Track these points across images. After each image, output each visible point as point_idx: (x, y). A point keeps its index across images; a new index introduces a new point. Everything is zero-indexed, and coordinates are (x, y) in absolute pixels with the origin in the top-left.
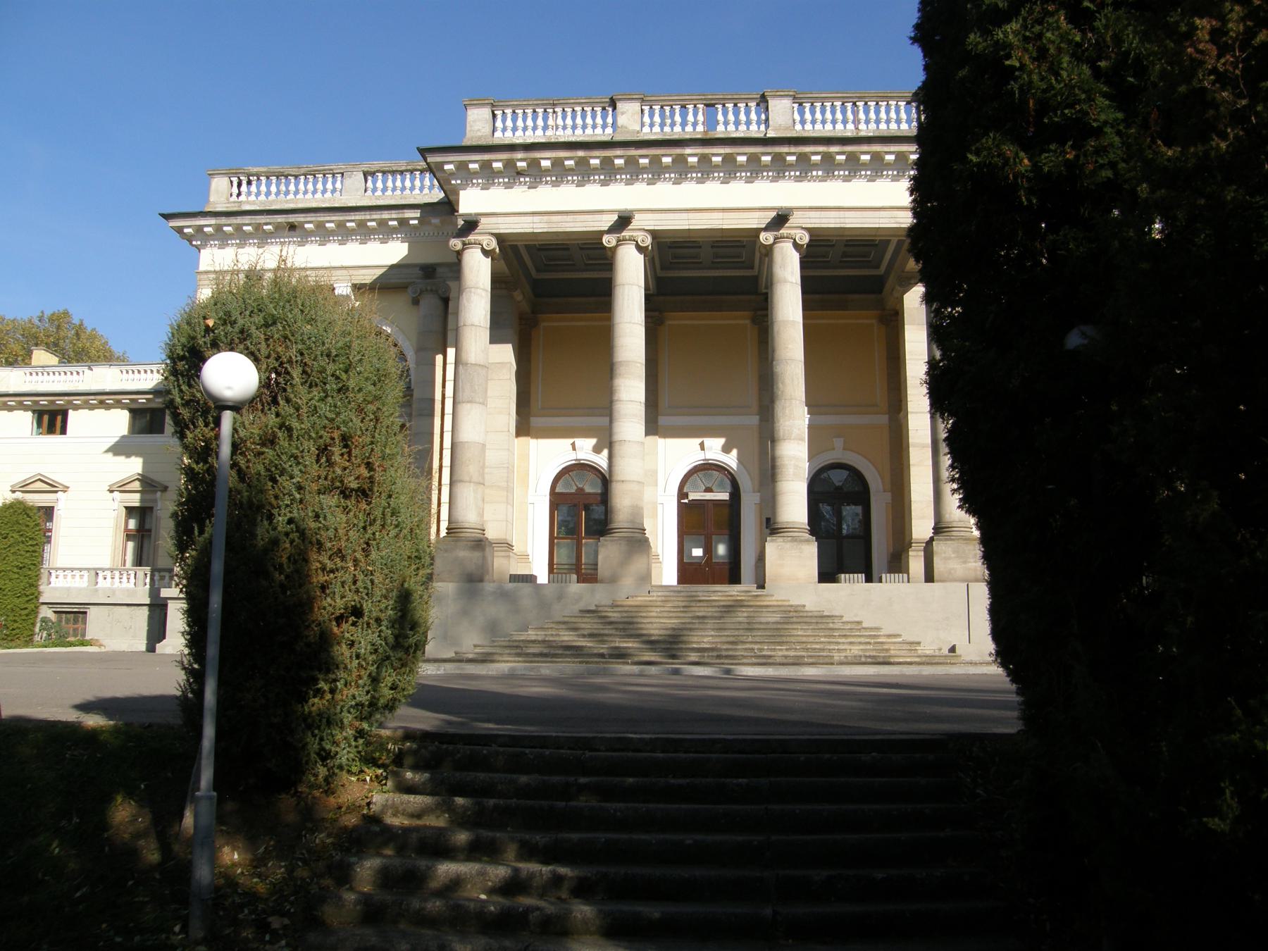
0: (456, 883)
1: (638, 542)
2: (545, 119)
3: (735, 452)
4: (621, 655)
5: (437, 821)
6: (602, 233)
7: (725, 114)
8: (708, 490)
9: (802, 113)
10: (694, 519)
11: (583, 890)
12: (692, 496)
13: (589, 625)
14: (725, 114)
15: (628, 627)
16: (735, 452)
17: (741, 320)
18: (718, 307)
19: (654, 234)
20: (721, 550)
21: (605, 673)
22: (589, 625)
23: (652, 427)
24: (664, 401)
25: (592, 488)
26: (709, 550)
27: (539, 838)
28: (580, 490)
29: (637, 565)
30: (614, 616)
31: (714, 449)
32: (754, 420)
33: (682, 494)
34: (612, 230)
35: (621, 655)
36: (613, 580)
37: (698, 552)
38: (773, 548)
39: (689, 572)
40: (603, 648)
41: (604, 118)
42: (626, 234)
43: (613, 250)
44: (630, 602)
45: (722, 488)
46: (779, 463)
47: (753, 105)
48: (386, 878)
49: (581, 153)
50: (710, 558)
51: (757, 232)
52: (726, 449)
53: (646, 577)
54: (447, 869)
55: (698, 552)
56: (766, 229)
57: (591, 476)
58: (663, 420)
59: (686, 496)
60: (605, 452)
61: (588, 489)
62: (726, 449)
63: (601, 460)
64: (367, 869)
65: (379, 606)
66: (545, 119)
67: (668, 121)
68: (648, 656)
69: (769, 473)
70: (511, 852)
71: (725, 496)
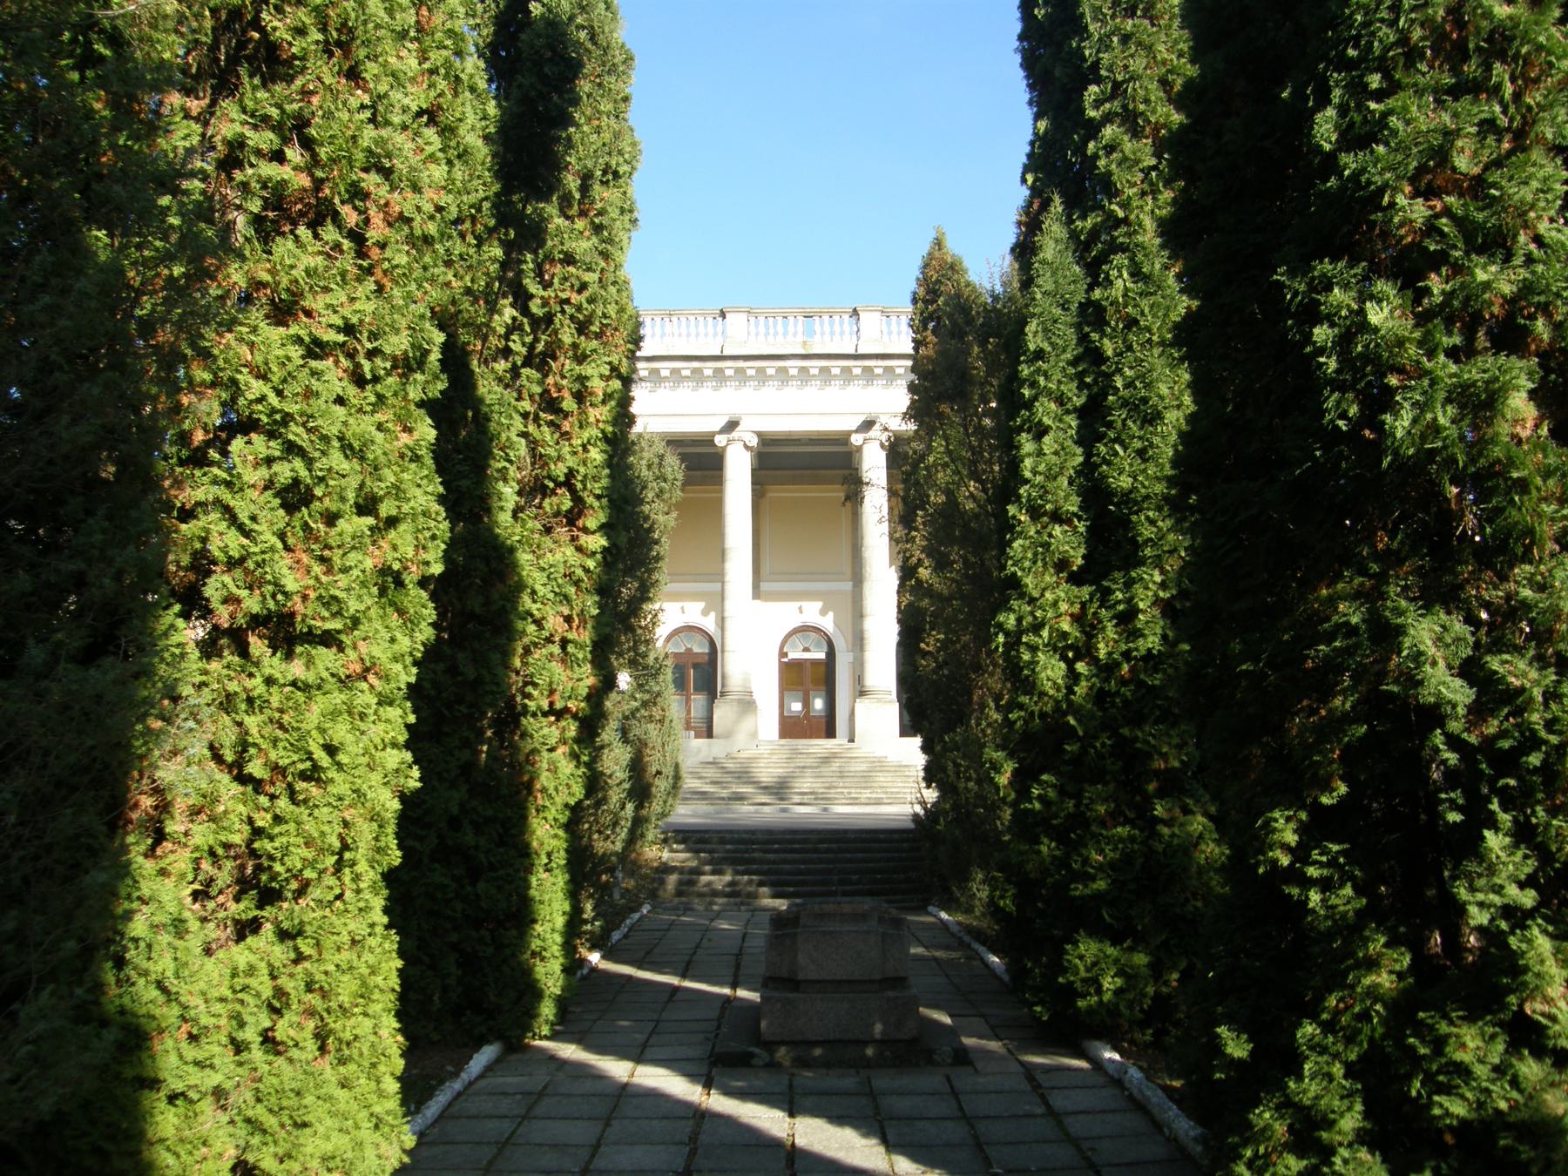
0: (709, 884)
1: (747, 704)
2: (663, 326)
3: (831, 615)
4: (740, 798)
5: (694, 864)
6: (713, 434)
7: (822, 324)
8: (806, 650)
9: (889, 325)
10: (795, 676)
11: (761, 884)
12: (792, 656)
13: (711, 773)
14: (822, 324)
15: (744, 775)
16: (831, 615)
17: (837, 493)
18: (816, 481)
19: (759, 434)
20: (818, 704)
21: (729, 811)
22: (711, 773)
23: (757, 594)
24: (766, 569)
25: (700, 648)
26: (807, 704)
27: (741, 868)
28: (689, 650)
29: (747, 725)
30: (730, 765)
31: (812, 613)
32: (849, 586)
33: (783, 654)
34: (722, 432)
35: (740, 798)
36: (728, 735)
37: (797, 707)
38: (862, 706)
39: (791, 728)
40: (724, 793)
41: (715, 326)
42: (735, 434)
43: (724, 449)
44: (742, 755)
45: (818, 645)
46: (867, 635)
47: (846, 317)
48: (680, 883)
49: (696, 364)
50: (808, 712)
51: (849, 433)
52: (823, 612)
53: (754, 735)
54: (705, 879)
55: (797, 707)
56: (856, 431)
57: (699, 637)
58: (764, 586)
59: (786, 655)
60: (713, 614)
61: (696, 650)
62: (823, 612)
63: (709, 623)
64: (672, 879)
65: (668, 771)
66: (663, 326)
67: (772, 331)
68: (764, 799)
69: (858, 641)
70: (730, 871)
71: (822, 656)
